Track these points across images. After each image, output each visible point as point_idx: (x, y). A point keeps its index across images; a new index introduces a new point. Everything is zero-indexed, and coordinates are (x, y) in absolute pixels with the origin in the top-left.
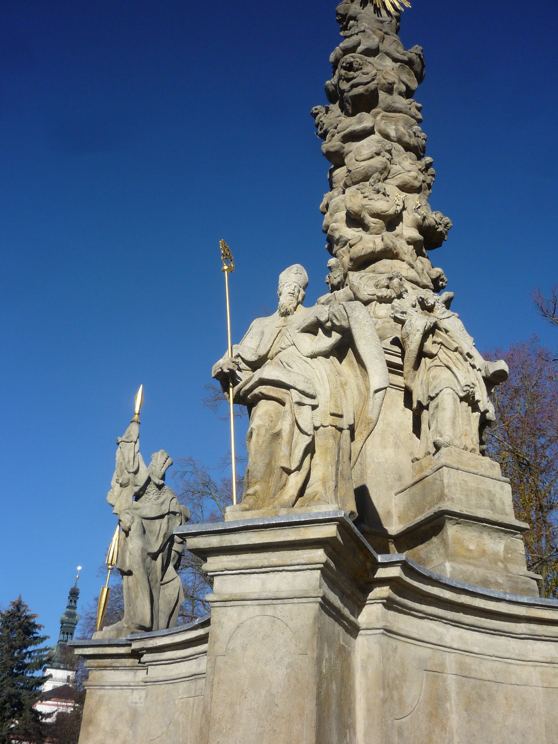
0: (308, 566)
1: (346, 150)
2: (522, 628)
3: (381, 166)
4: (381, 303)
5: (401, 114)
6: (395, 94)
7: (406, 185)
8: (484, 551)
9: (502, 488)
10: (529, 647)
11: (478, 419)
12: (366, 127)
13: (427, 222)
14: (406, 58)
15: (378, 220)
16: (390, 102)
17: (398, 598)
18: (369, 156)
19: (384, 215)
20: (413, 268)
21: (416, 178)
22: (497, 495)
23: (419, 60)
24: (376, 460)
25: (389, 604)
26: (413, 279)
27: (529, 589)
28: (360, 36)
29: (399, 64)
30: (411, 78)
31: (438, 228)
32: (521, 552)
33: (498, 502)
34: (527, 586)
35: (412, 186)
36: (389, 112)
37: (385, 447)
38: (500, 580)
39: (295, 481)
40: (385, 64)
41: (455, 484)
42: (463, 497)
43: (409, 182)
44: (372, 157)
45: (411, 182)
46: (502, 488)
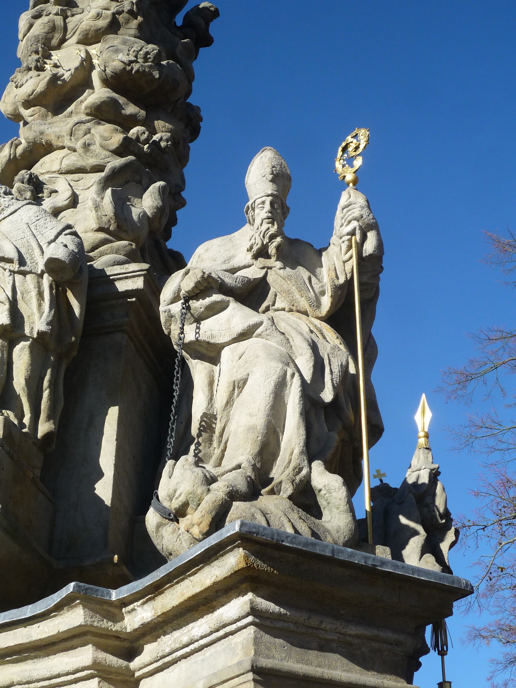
3: (43, 31)
7: (87, 34)
13: (108, 71)
15: (32, 109)
19: (34, 99)
20: (75, 151)
21: (98, 16)
26: (70, 168)
31: (132, 69)
35: (97, 31)
43: (88, 27)
44: (31, 26)
45: (91, 26)
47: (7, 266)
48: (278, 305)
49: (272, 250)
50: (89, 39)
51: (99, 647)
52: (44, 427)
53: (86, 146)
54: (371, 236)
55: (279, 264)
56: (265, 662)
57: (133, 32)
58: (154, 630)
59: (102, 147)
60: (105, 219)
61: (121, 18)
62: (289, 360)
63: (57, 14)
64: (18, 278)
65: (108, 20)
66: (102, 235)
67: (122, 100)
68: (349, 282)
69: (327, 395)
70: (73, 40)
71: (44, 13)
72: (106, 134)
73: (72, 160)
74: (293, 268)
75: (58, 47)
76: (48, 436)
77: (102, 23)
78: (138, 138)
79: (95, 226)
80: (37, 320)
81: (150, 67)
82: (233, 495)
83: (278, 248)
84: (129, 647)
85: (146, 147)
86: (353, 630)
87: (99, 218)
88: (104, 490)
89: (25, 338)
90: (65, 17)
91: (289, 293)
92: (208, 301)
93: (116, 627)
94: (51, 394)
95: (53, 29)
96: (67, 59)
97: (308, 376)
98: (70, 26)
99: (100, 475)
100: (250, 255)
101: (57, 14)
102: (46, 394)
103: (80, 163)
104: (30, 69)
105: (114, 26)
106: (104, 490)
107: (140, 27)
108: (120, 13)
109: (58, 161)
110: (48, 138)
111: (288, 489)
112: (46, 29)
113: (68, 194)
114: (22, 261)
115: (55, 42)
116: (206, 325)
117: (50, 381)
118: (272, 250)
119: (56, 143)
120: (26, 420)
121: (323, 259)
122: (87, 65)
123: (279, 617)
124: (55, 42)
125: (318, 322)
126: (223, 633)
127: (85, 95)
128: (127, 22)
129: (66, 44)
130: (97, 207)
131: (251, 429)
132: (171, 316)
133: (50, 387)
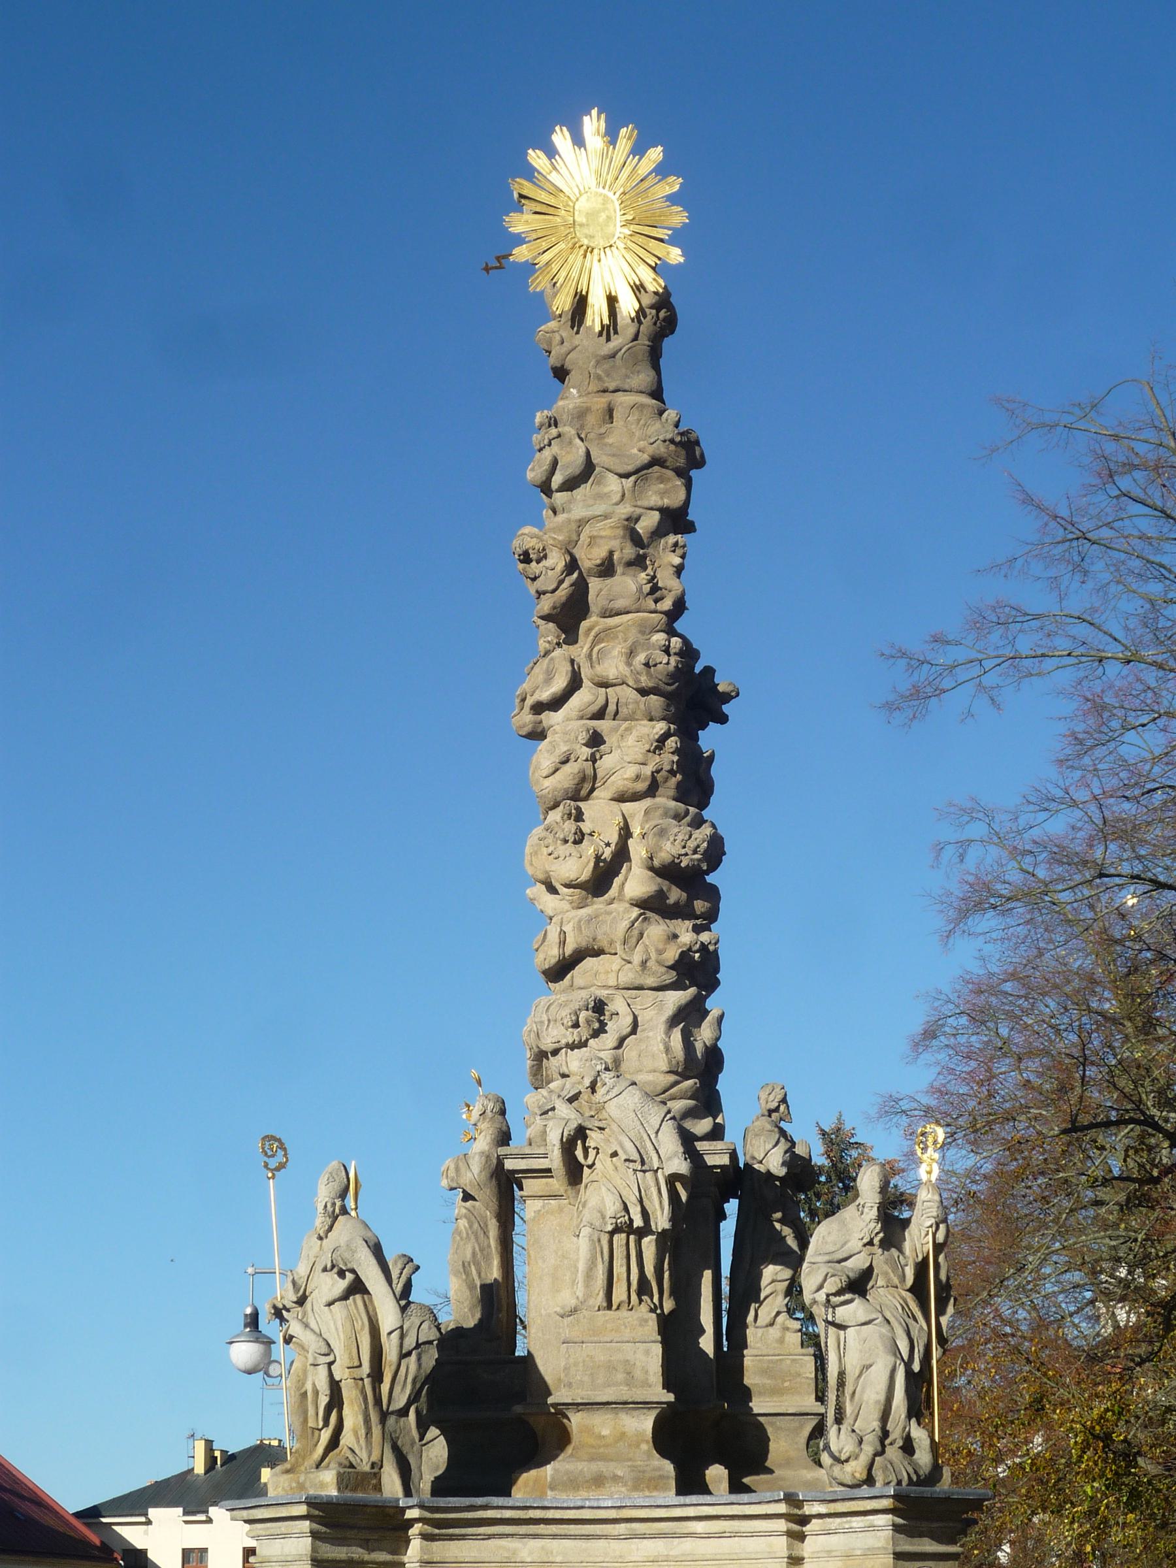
0: (300, 1535)
1: (545, 724)
2: (622, 1528)
4: (572, 1050)
5: (630, 616)
6: (619, 569)
8: (623, 1434)
9: (647, 1352)
10: (633, 1547)
11: (654, 1244)
12: (554, 694)
14: (645, 458)
16: (605, 603)
17: (437, 1531)
18: (551, 771)
21: (638, 777)
22: (638, 1364)
23: (672, 447)
24: (543, 1312)
25: (426, 1537)
27: (661, 1477)
28: (555, 449)
29: (632, 478)
30: (670, 485)
32: (808, 1375)
33: (638, 1374)
34: (657, 1474)
36: (610, 616)
37: (558, 1291)
38: (620, 1473)
39: (326, 1435)
40: (606, 490)
41: (576, 1364)
42: (586, 1378)
44: (557, 770)
46: (647, 1352)
47: (631, 1165)
48: (880, 1283)
49: (876, 1241)
50: (622, 798)
51: (787, 1520)
52: (668, 1305)
53: (644, 963)
54: (942, 1226)
55: (880, 1251)
56: (899, 1549)
57: (672, 792)
58: (820, 1516)
59: (659, 963)
60: (674, 1062)
61: (659, 777)
62: (896, 1351)
63: (587, 760)
64: (640, 1174)
65: (647, 783)
66: (672, 1078)
67: (665, 884)
68: (925, 1260)
69: (916, 1367)
70: (602, 794)
71: (572, 758)
72: (661, 946)
73: (628, 976)
74: (888, 1250)
75: (587, 798)
76: (671, 1312)
77: (642, 786)
78: (690, 949)
79: (665, 1068)
80: (662, 1220)
81: (699, 860)
82: (876, 1455)
83: (881, 1241)
84: (804, 1520)
85: (697, 955)
86: (935, 1525)
87: (670, 1062)
88: (707, 1343)
89: (651, 1232)
90: (594, 761)
91: (886, 1273)
92: (842, 1298)
93: (800, 1512)
94: (671, 1275)
95: (583, 779)
96: (602, 817)
97: (906, 1358)
98: (600, 774)
99: (702, 1331)
100: (861, 1243)
101: (587, 760)
102: (666, 1275)
103: (638, 982)
104: (566, 841)
105: (652, 790)
106: (707, 1343)
107: (679, 786)
108: (658, 771)
109: (614, 975)
110: (601, 944)
111: (900, 1443)
112: (576, 781)
113: (630, 1019)
114: (643, 1163)
115: (583, 793)
116: (839, 1310)
117: (669, 1264)
118: (876, 1241)
119: (607, 950)
120: (656, 1299)
121: (906, 1233)
122: (625, 833)
123: (904, 1525)
124: (583, 793)
125: (904, 1293)
126: (872, 1528)
127: (623, 871)
128: (666, 780)
129: (595, 794)
130: (667, 1049)
131: (877, 1402)
132: (815, 1302)
133: (670, 1269)
